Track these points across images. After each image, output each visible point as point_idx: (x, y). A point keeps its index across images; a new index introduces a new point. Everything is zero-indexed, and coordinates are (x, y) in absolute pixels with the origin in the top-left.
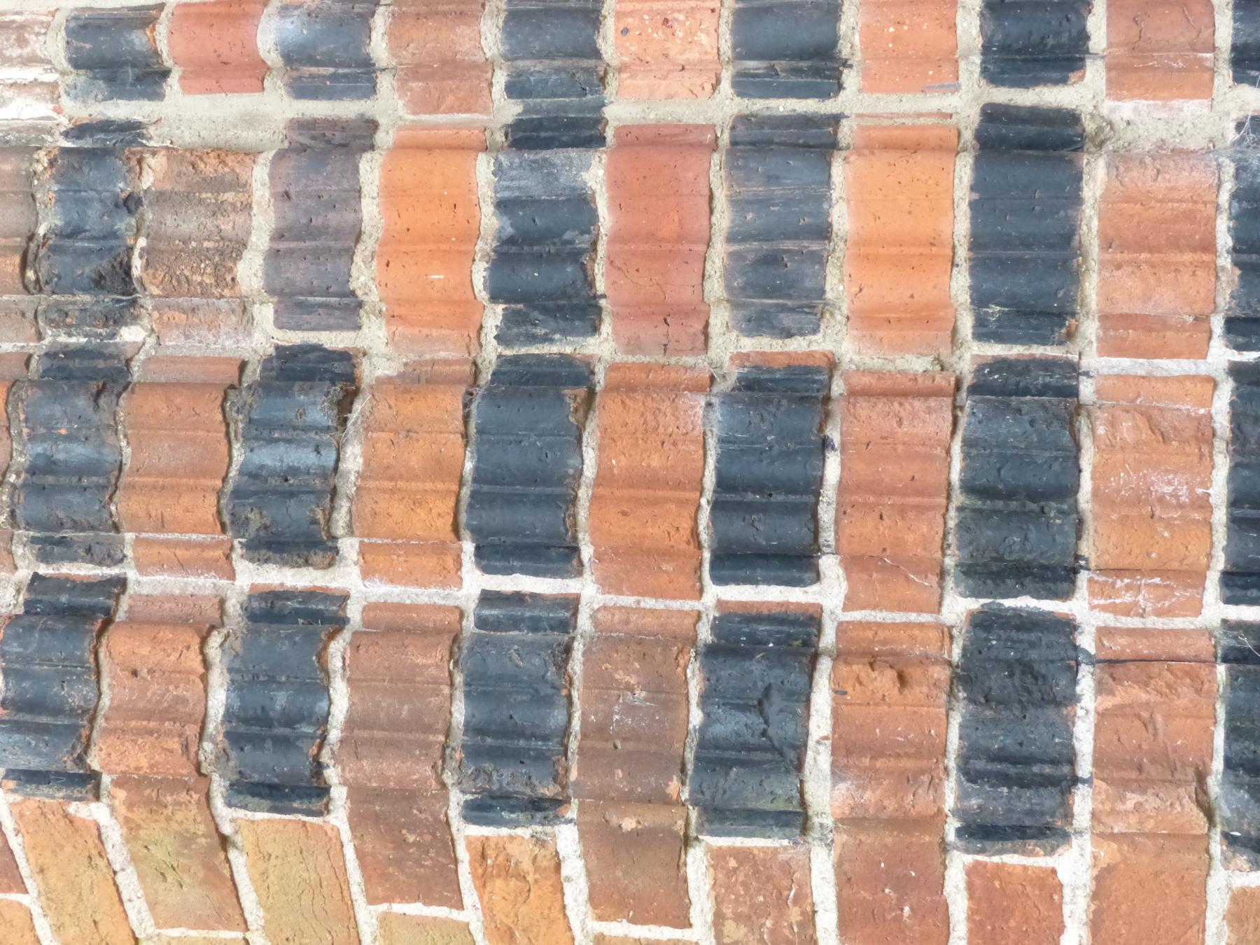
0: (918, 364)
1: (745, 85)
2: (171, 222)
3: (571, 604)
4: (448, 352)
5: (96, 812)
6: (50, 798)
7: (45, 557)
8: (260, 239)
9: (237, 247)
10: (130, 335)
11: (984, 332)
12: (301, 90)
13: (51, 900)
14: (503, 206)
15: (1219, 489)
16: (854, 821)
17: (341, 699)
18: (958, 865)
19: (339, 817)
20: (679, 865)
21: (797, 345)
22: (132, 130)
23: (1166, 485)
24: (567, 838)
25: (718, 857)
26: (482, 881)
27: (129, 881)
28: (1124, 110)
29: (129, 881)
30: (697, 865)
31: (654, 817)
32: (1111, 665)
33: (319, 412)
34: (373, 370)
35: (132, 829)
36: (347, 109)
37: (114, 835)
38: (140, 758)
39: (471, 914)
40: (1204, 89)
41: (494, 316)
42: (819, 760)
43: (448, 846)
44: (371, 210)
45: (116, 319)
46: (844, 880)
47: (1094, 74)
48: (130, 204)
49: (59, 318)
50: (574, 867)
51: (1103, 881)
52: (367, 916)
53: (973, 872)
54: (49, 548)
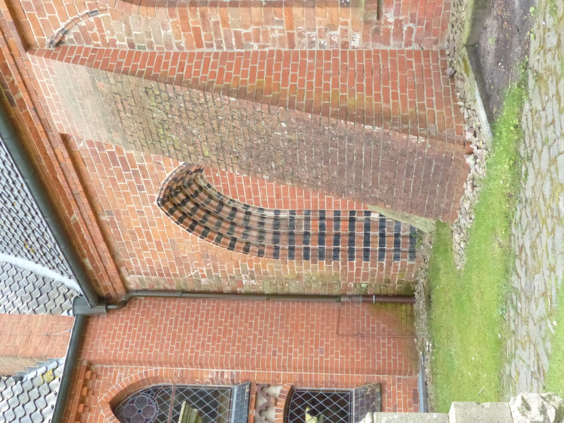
0: (345, 233)
1: (334, 215)
4: (316, 232)
8: (303, 225)
9: (302, 226)
15: (363, 240)
17: (310, 254)
22: (293, 217)
23: (360, 241)
24: (325, 261)
30: (332, 262)
32: (357, 251)
33: (308, 237)
34: (311, 233)
38: (298, 258)
39: (318, 265)
42: (340, 257)
44: (311, 224)
51: (356, 263)
52: (311, 265)
54: (290, 244)
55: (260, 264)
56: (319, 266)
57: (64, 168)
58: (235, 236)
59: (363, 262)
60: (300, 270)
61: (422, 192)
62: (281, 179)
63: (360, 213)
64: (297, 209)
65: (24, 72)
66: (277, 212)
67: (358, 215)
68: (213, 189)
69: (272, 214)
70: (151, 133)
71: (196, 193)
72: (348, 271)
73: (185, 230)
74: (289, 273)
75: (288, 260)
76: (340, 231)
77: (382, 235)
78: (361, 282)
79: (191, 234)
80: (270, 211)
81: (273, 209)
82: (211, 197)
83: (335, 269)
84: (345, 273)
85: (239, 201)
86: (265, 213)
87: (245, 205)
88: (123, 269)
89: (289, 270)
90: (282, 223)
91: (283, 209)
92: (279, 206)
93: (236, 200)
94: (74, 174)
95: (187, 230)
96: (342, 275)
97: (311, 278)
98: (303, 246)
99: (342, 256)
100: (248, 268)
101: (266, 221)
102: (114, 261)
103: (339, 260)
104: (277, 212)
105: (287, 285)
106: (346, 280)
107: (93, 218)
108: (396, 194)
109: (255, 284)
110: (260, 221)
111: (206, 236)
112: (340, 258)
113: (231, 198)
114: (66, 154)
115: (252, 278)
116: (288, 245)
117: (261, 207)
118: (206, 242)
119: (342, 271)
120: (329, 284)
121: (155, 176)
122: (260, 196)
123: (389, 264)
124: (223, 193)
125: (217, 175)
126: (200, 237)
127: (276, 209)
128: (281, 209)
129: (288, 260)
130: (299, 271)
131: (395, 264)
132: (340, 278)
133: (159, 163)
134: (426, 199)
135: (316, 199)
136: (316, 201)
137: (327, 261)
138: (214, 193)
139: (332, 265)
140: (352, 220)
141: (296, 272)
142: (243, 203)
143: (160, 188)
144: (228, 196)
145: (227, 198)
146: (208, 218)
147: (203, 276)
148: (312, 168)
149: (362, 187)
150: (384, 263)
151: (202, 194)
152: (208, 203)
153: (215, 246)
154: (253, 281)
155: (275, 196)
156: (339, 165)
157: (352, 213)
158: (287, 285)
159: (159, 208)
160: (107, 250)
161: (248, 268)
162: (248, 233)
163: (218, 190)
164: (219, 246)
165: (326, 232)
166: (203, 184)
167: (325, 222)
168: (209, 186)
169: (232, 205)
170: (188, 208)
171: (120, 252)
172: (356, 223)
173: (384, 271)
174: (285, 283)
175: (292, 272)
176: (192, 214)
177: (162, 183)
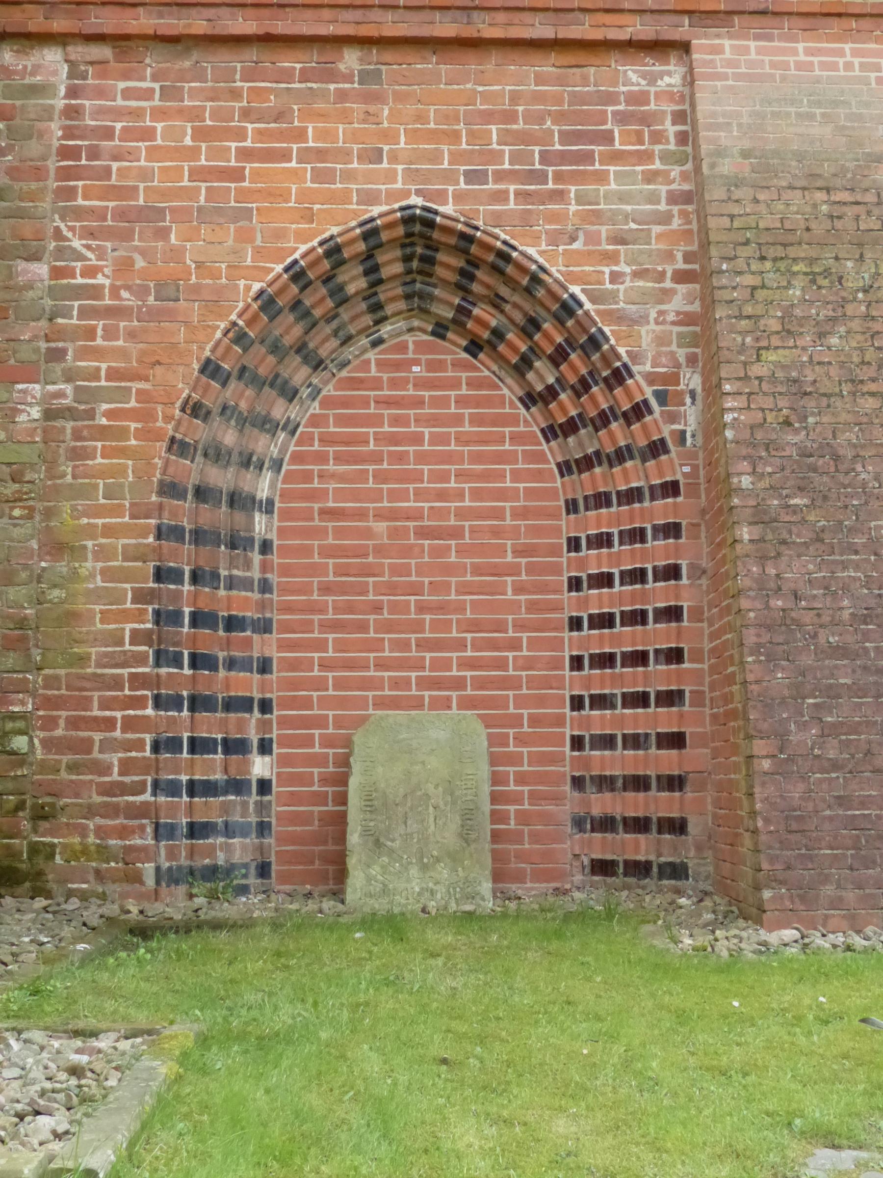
1: (258, 658)
2: (242, 557)
3: (182, 626)
5: (151, 539)
6: (154, 530)
7: (190, 531)
10: (223, 547)
11: (223, 698)
12: (259, 580)
13: (126, 524)
14: (244, 617)
16: (158, 675)
18: (149, 693)
19: (151, 585)
20: (145, 645)
21: (221, 666)
24: (149, 626)
25: (147, 652)
26: (139, 609)
27: (133, 541)
28: (253, 721)
29: (133, 541)
30: (144, 648)
31: (156, 642)
35: (148, 545)
36: (256, 588)
37: (145, 541)
38: (165, 551)
39: (128, 605)
40: (257, 733)
41: (226, 614)
43: (147, 603)
45: (226, 546)
46: (143, 674)
47: (260, 716)
48: (245, 550)
49: (226, 535)
50: (142, 626)
53: (147, 696)
55: (133, 442)
56: (125, 611)
57: (570, 16)
58: (233, 384)
59: (148, 738)
60: (101, 553)
61: (858, 836)
62: (754, 515)
63: (264, 726)
64: (276, 561)
65: (865, 24)
66: (268, 507)
67: (258, 720)
68: (364, 351)
69: (263, 491)
70: (785, 245)
71: (376, 307)
72: (96, 694)
73: (297, 255)
74: (85, 521)
75: (153, 521)
76: (222, 673)
77: (209, 789)
78: (42, 734)
79: (279, 268)
80: (273, 485)
81: (277, 499)
82: (347, 340)
83: (106, 654)
84: (88, 685)
85: (311, 411)
86: (268, 476)
87: (298, 425)
88: (104, 52)
89: (100, 521)
90: (239, 517)
91: (276, 523)
92: (286, 514)
93: (316, 404)
94: (545, 32)
95: (296, 262)
96: (83, 677)
97: (55, 586)
98: (187, 569)
99: (169, 674)
100: (105, 406)
101: (249, 475)
102: (144, 37)
103: (158, 664)
104: (268, 507)
105: (17, 513)
106: (45, 687)
107: (364, 31)
108: (821, 781)
109: (22, 418)
110: (254, 459)
111: (262, 308)
112: (164, 671)
113: (324, 393)
114: (613, 34)
115: (49, 414)
116: (188, 527)
117: (285, 467)
118: (241, 305)
119: (95, 675)
120: (24, 639)
121: (526, 220)
122: (331, 467)
123: (142, 811)
124: (344, 373)
125: (416, 369)
126: (261, 292)
127: (277, 505)
128: (276, 515)
129: (153, 521)
130: (94, 552)
131: (142, 828)
132: (62, 672)
133: (573, 239)
134: (832, 849)
135: (322, 611)
136: (312, 611)
137: (149, 632)
138: (350, 352)
139: (127, 647)
140: (245, 704)
141: (90, 544)
142: (303, 422)
143: (480, 223)
144: (330, 386)
145: (326, 383)
146: (302, 323)
147: (57, 273)
148: (826, 588)
149: (811, 701)
150: (147, 797)
151: (368, 320)
152: (335, 333)
153: (223, 325)
154: (35, 413)
155: (331, 504)
156: (865, 648)
157: (265, 706)
158: (17, 513)
159: (396, 206)
160: (218, 31)
161: (105, 406)
162: (233, 422)
163: (355, 363)
164: (218, 334)
165: (221, 633)
166: (386, 329)
167: (249, 633)
168: (375, 344)
169: (305, 392)
170: (353, 279)
171: (187, 64)
172: (247, 715)
173: (98, 799)
174: (31, 509)
175: (90, 532)
176: (331, 285)
177: (497, 231)
